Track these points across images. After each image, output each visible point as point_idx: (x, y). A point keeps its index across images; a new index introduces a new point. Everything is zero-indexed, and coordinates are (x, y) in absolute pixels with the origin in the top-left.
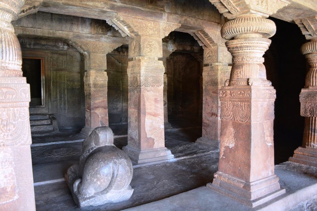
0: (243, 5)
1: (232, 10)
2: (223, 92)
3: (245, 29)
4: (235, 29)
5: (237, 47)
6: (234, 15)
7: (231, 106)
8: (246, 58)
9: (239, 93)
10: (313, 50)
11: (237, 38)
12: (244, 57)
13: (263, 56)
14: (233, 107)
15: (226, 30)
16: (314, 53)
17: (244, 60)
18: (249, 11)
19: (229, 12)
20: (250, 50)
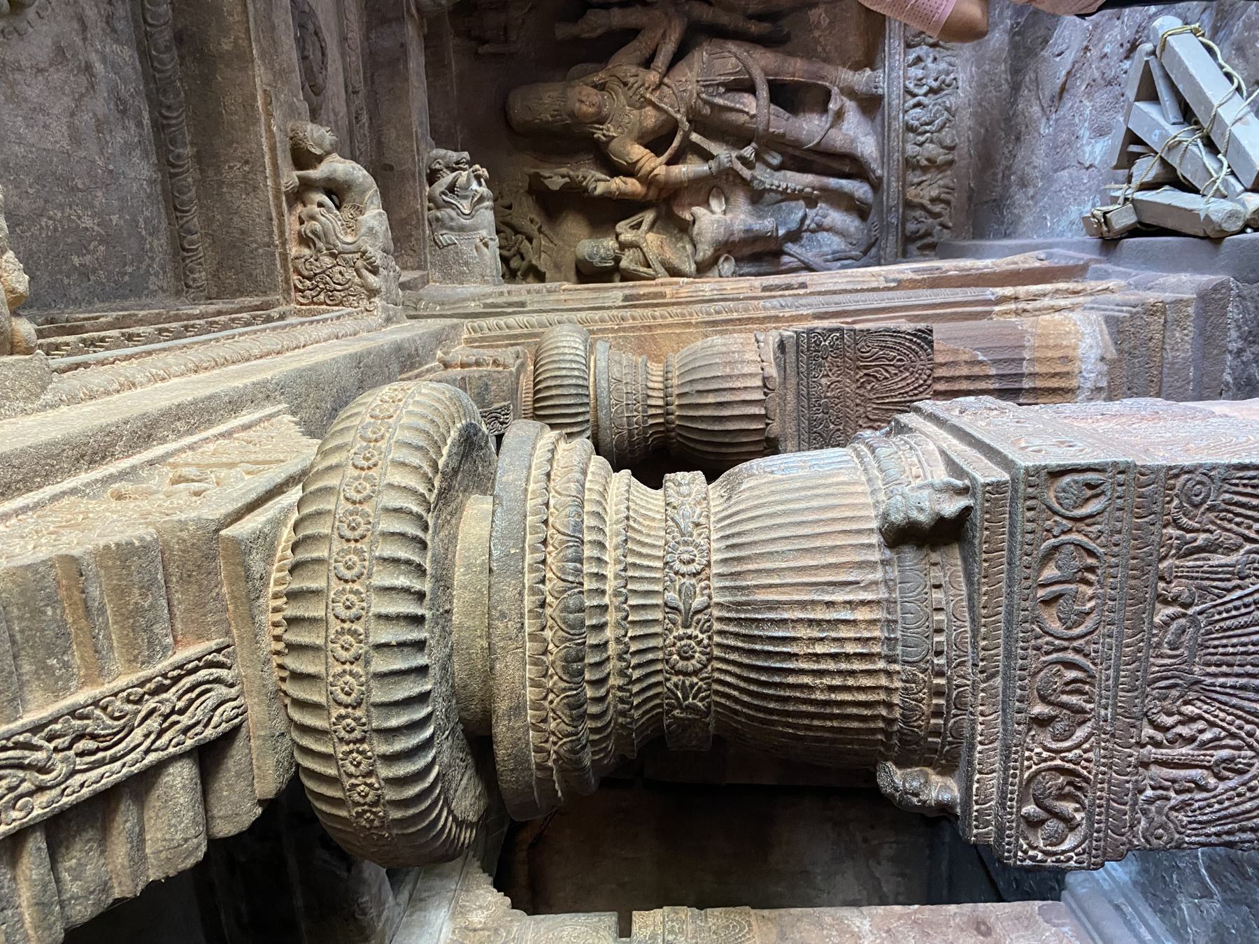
0: (146, 589)
1: (185, 720)
2: (1034, 824)
3: (396, 561)
4: (382, 664)
5: (573, 664)
6: (257, 713)
7: (1192, 719)
8: (679, 581)
9: (1056, 626)
10: (580, 419)
11: (475, 686)
12: (671, 596)
13: (656, 484)
14: (1207, 694)
15: (385, 772)
16: (597, 426)
17: (698, 602)
18: (240, 550)
19: (209, 757)
20: (601, 545)
